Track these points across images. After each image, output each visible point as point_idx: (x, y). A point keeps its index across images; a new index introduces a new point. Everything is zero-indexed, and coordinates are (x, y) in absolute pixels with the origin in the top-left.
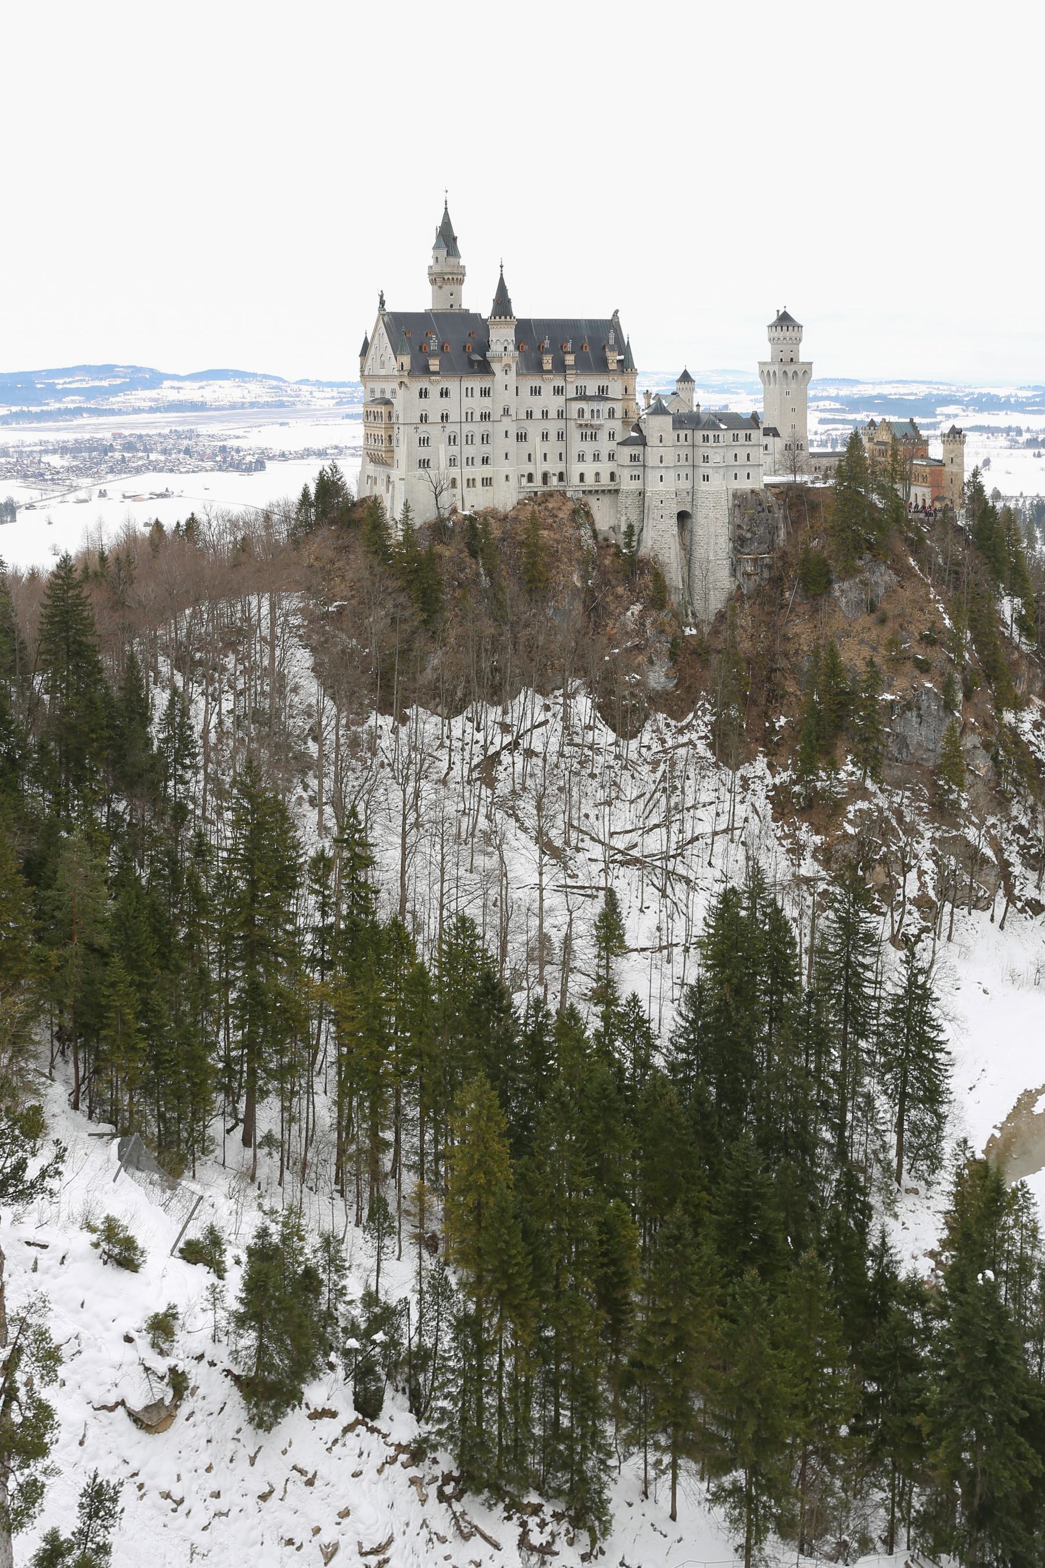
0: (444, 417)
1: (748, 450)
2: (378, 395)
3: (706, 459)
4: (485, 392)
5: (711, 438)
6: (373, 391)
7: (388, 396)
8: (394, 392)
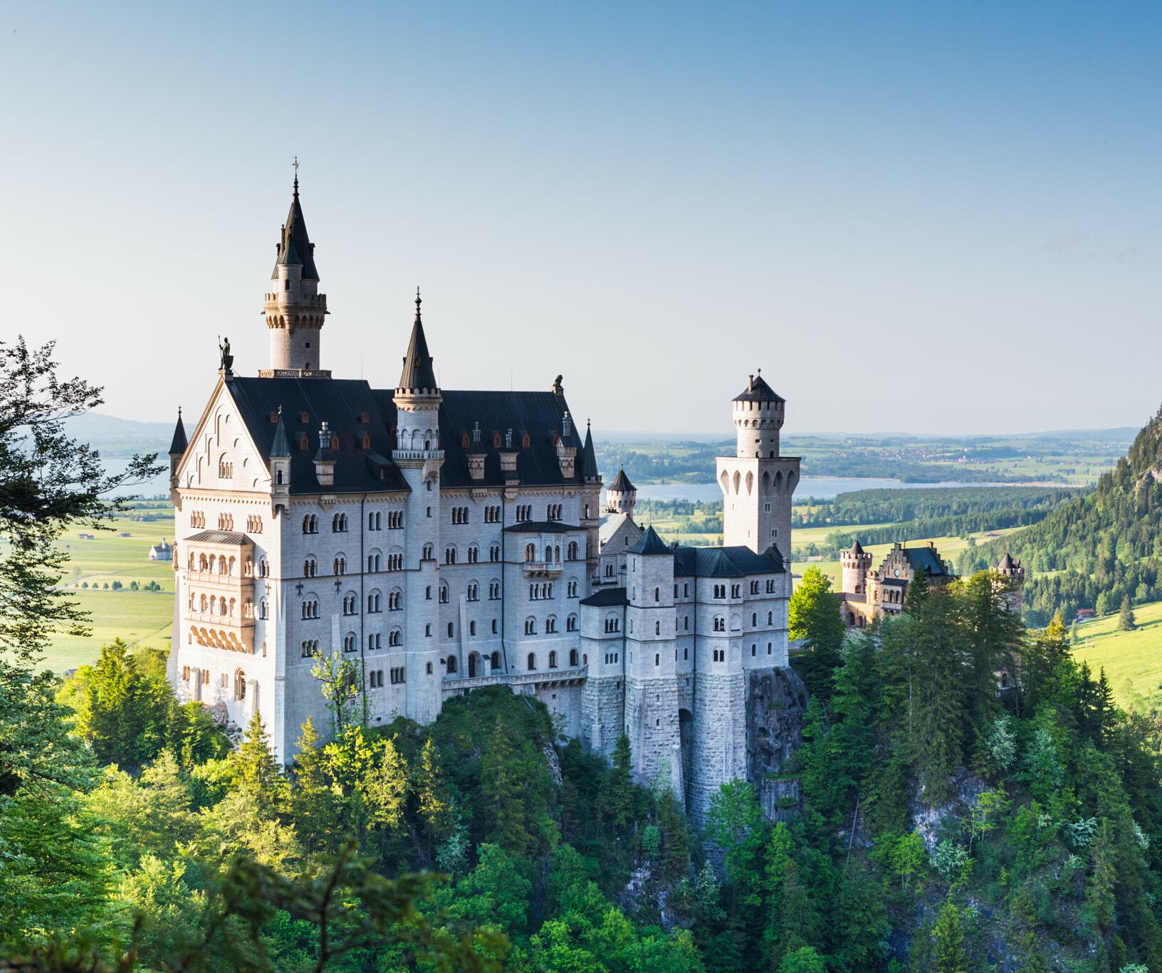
0: (340, 565)
1: (770, 607)
2: (212, 525)
3: (719, 626)
4: (396, 521)
5: (728, 590)
6: (196, 520)
7: (240, 528)
8: (254, 524)
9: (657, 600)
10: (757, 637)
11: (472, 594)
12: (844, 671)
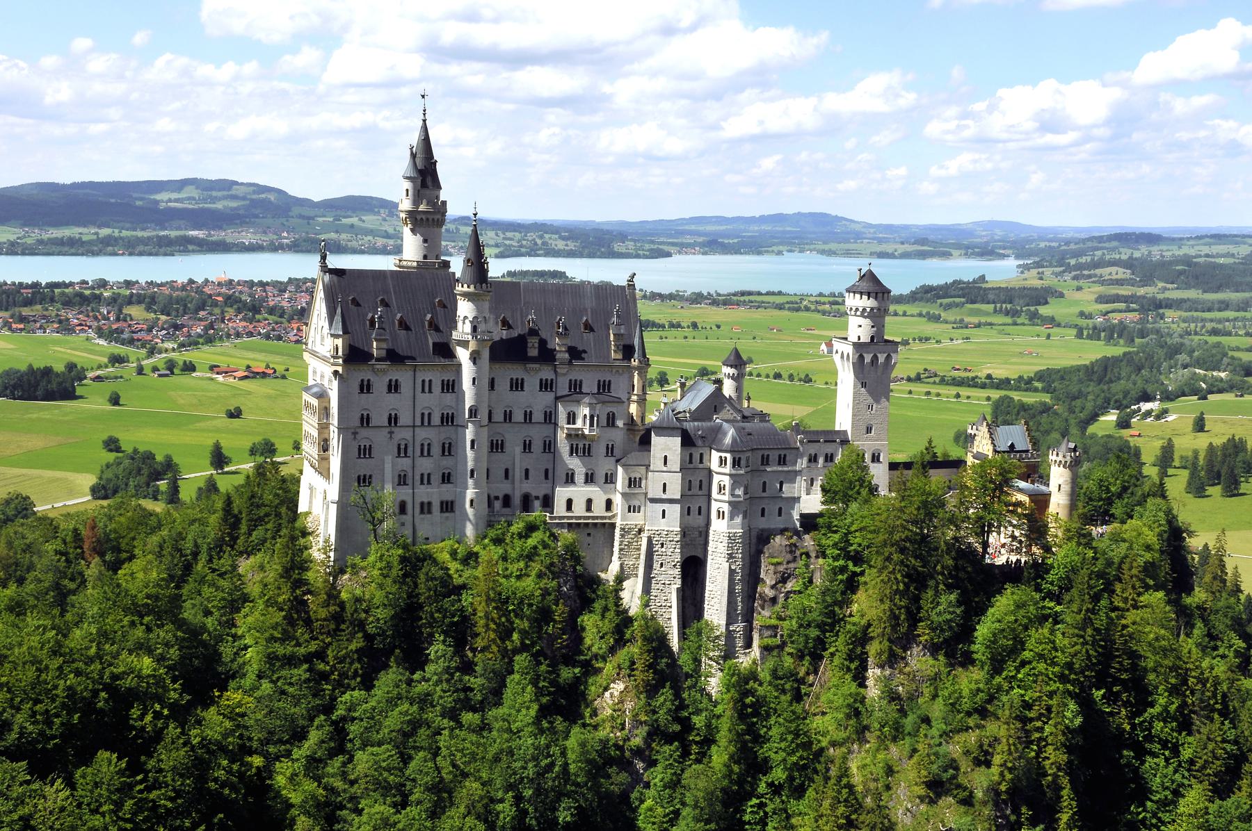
9: (665, 463)
10: (766, 501)
11: (527, 447)
12: (837, 537)
